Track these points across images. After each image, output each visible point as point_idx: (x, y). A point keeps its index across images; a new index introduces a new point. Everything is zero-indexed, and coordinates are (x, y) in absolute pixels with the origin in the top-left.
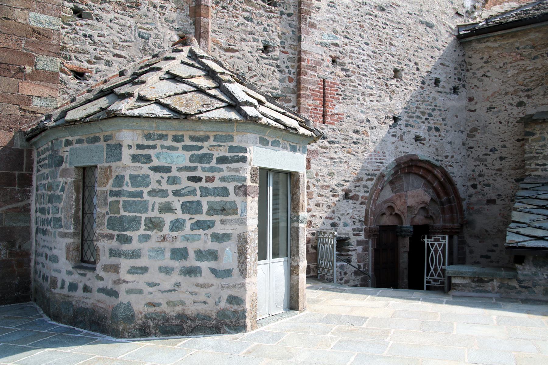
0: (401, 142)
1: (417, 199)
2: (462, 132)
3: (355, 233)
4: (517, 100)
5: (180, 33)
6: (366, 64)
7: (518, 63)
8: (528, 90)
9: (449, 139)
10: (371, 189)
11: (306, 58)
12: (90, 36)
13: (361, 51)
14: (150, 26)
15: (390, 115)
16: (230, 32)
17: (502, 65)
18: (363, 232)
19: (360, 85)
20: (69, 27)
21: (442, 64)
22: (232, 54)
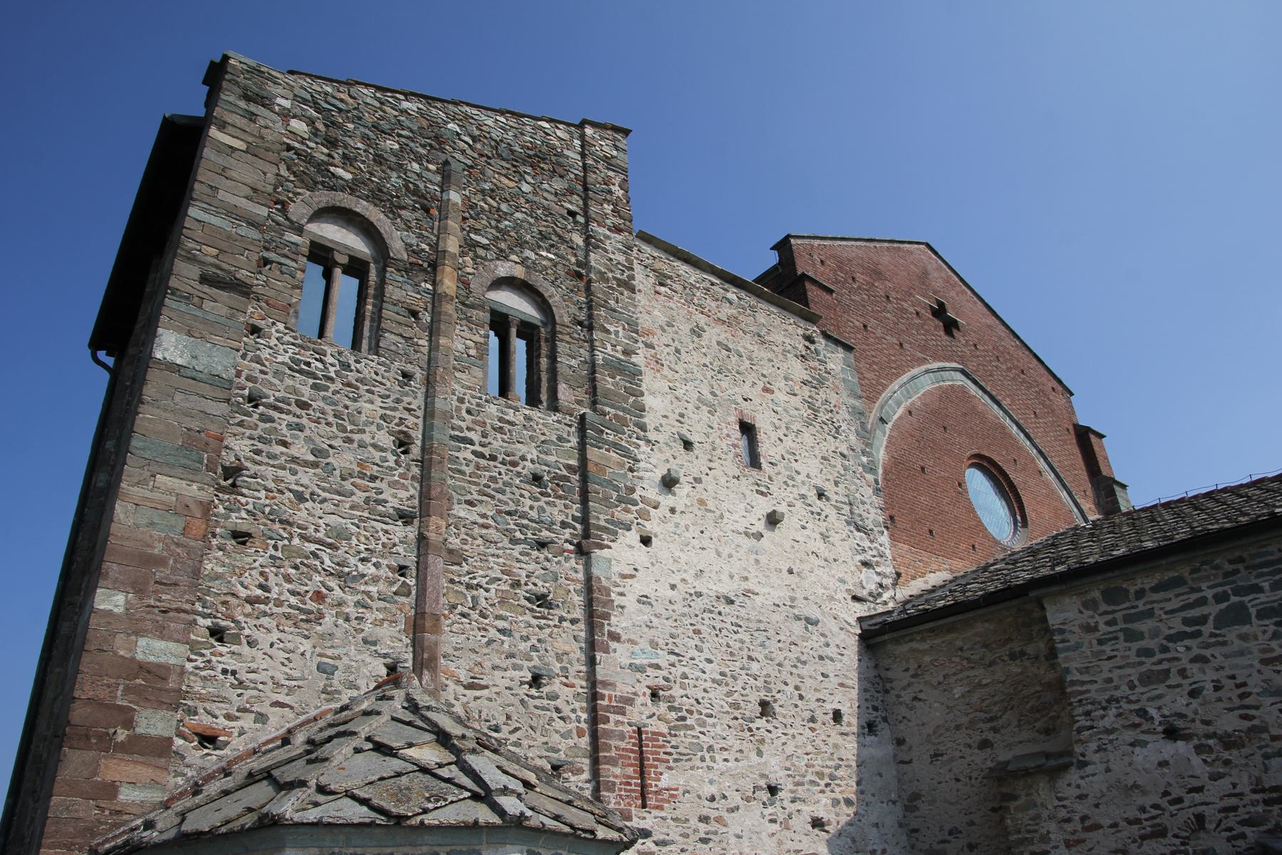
0: (789, 834)
2: (894, 803)
4: (977, 738)
5: (389, 661)
6: (710, 695)
7: (967, 673)
8: (991, 720)
9: (873, 819)
11: (606, 692)
12: (234, 673)
13: (700, 674)
14: (336, 652)
15: (762, 783)
16: (474, 656)
17: (941, 679)
19: (703, 733)
20: (200, 659)
21: (842, 685)
22: (478, 693)
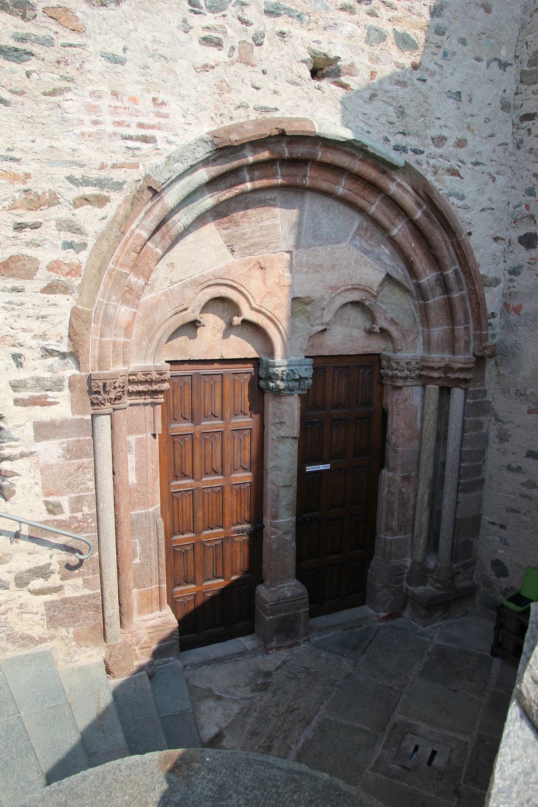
0: (245, 72)
1: (332, 278)
2: (503, 65)
3: (24, 395)
9: (453, 83)
10: (101, 237)
18: (66, 391)
